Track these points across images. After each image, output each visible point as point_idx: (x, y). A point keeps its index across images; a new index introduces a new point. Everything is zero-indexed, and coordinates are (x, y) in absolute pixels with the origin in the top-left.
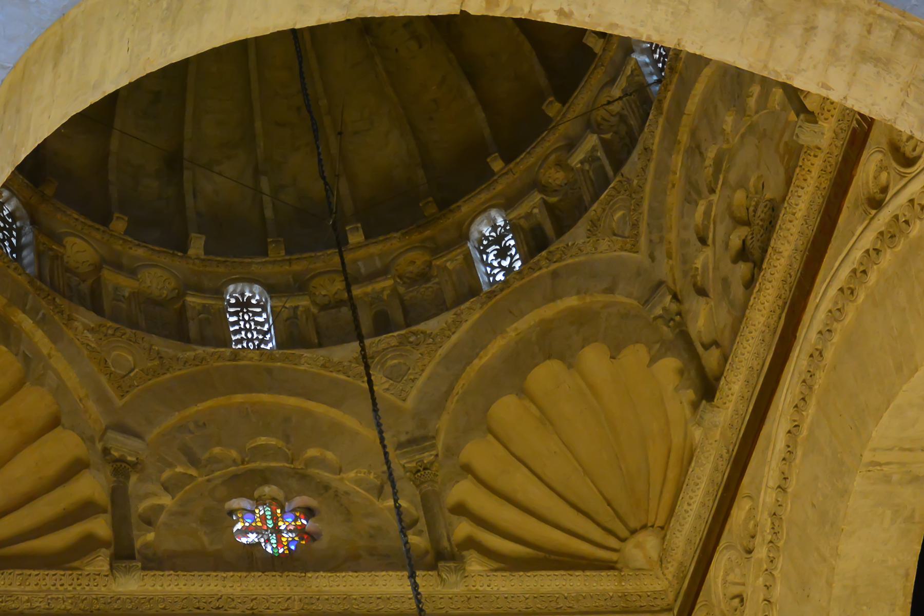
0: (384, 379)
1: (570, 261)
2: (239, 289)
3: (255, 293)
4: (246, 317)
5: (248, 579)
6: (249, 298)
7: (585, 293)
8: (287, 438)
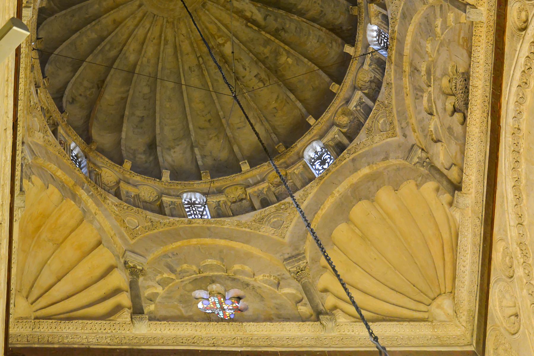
0: (271, 229)
1: (360, 152)
2: (189, 197)
3: (197, 198)
4: (194, 209)
5: (209, 326)
6: (194, 201)
7: (373, 164)
8: (222, 260)
